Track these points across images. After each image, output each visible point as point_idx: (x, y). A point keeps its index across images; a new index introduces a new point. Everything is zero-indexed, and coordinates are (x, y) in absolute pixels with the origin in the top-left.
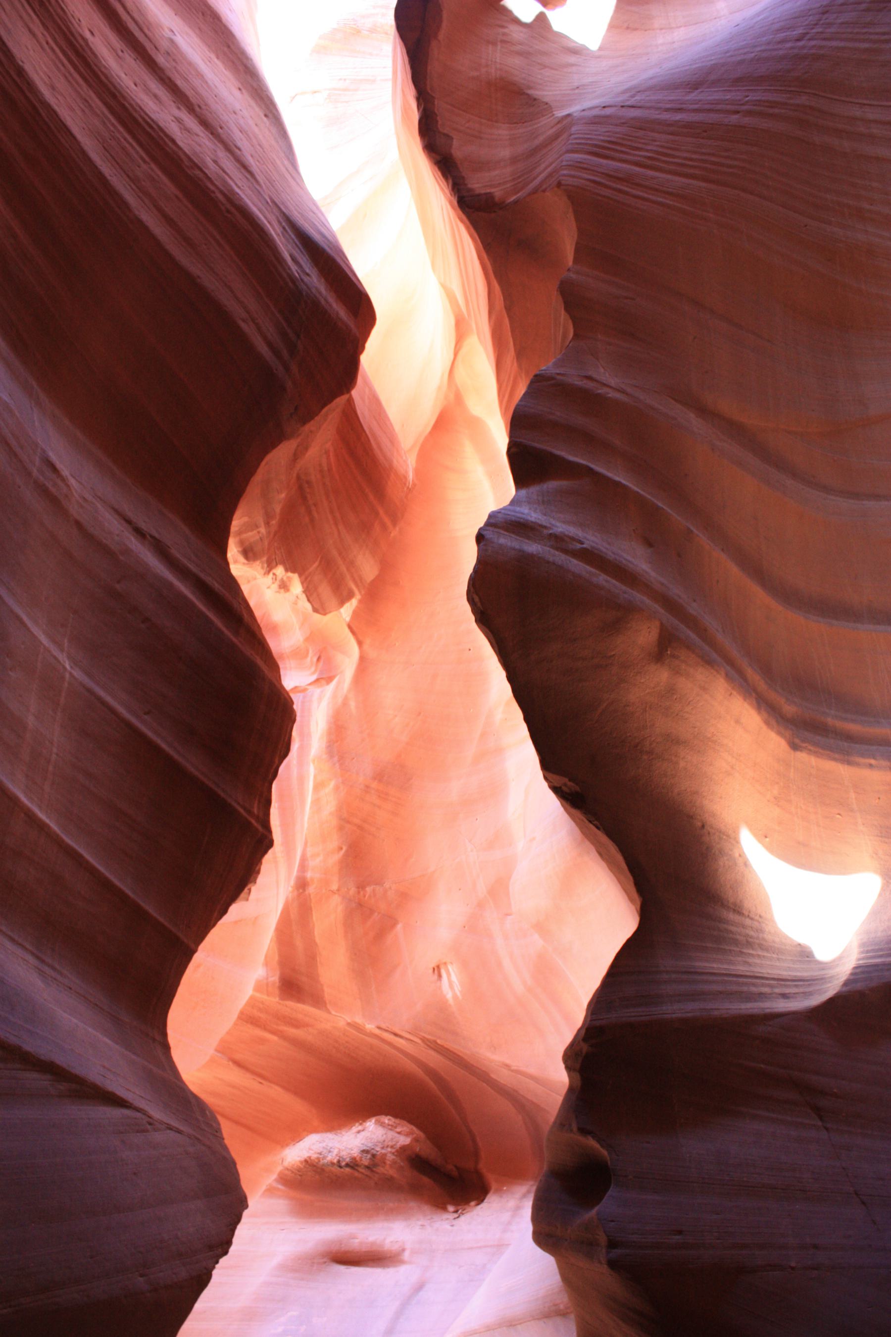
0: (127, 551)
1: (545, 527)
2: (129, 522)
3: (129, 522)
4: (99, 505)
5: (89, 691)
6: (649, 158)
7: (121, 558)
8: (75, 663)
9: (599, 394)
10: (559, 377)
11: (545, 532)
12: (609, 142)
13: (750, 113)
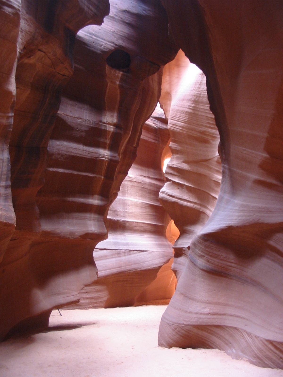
0: (143, 181)
1: (165, 192)
2: (143, 176)
3: (143, 176)
4: (137, 176)
5: (142, 202)
6: (178, 119)
7: (142, 182)
8: (139, 199)
9: (173, 167)
10: (169, 165)
11: (165, 192)
12: (174, 116)
13: (188, 108)
